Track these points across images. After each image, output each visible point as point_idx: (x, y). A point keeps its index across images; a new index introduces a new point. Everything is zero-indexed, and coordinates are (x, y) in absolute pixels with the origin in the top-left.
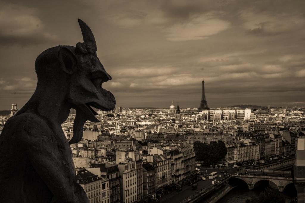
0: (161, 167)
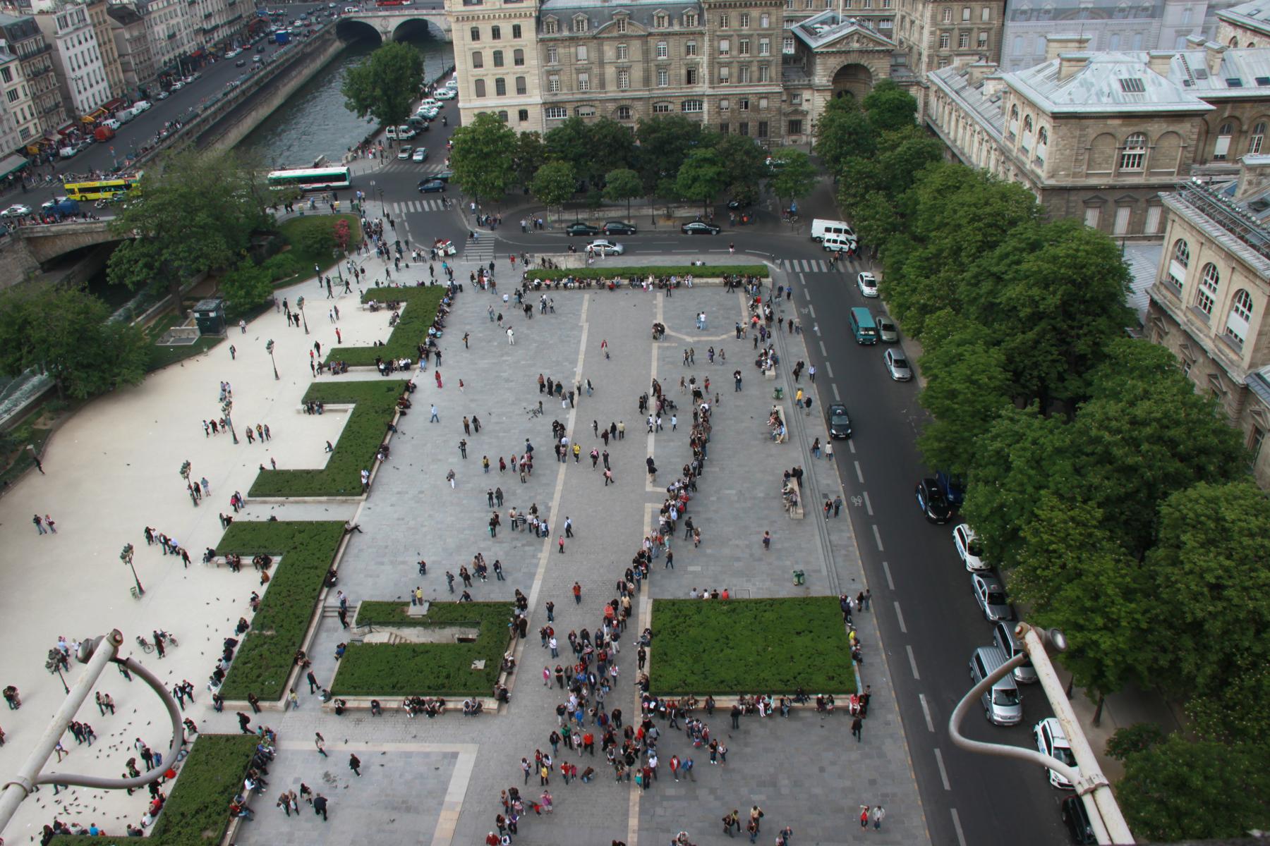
0: (162, 13)
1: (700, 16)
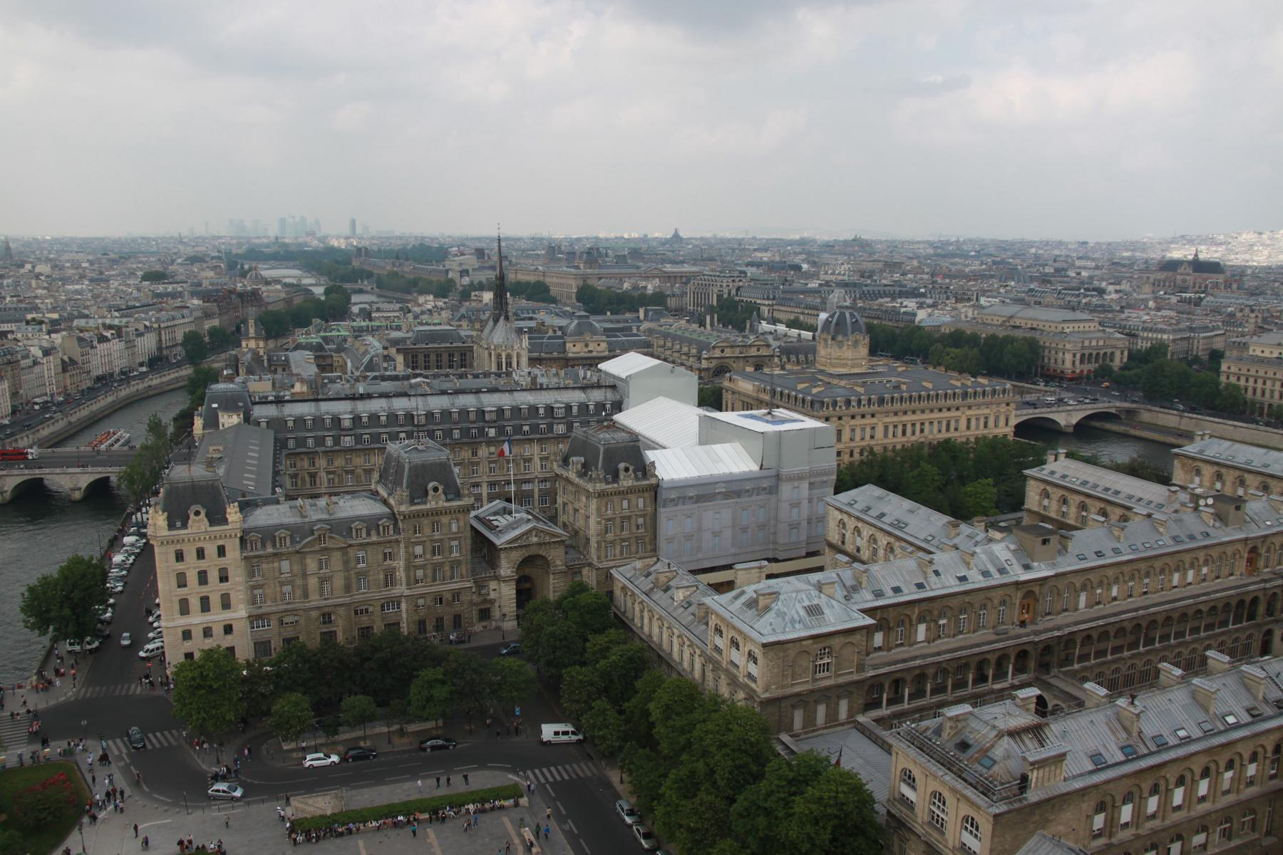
1: (396, 524)
